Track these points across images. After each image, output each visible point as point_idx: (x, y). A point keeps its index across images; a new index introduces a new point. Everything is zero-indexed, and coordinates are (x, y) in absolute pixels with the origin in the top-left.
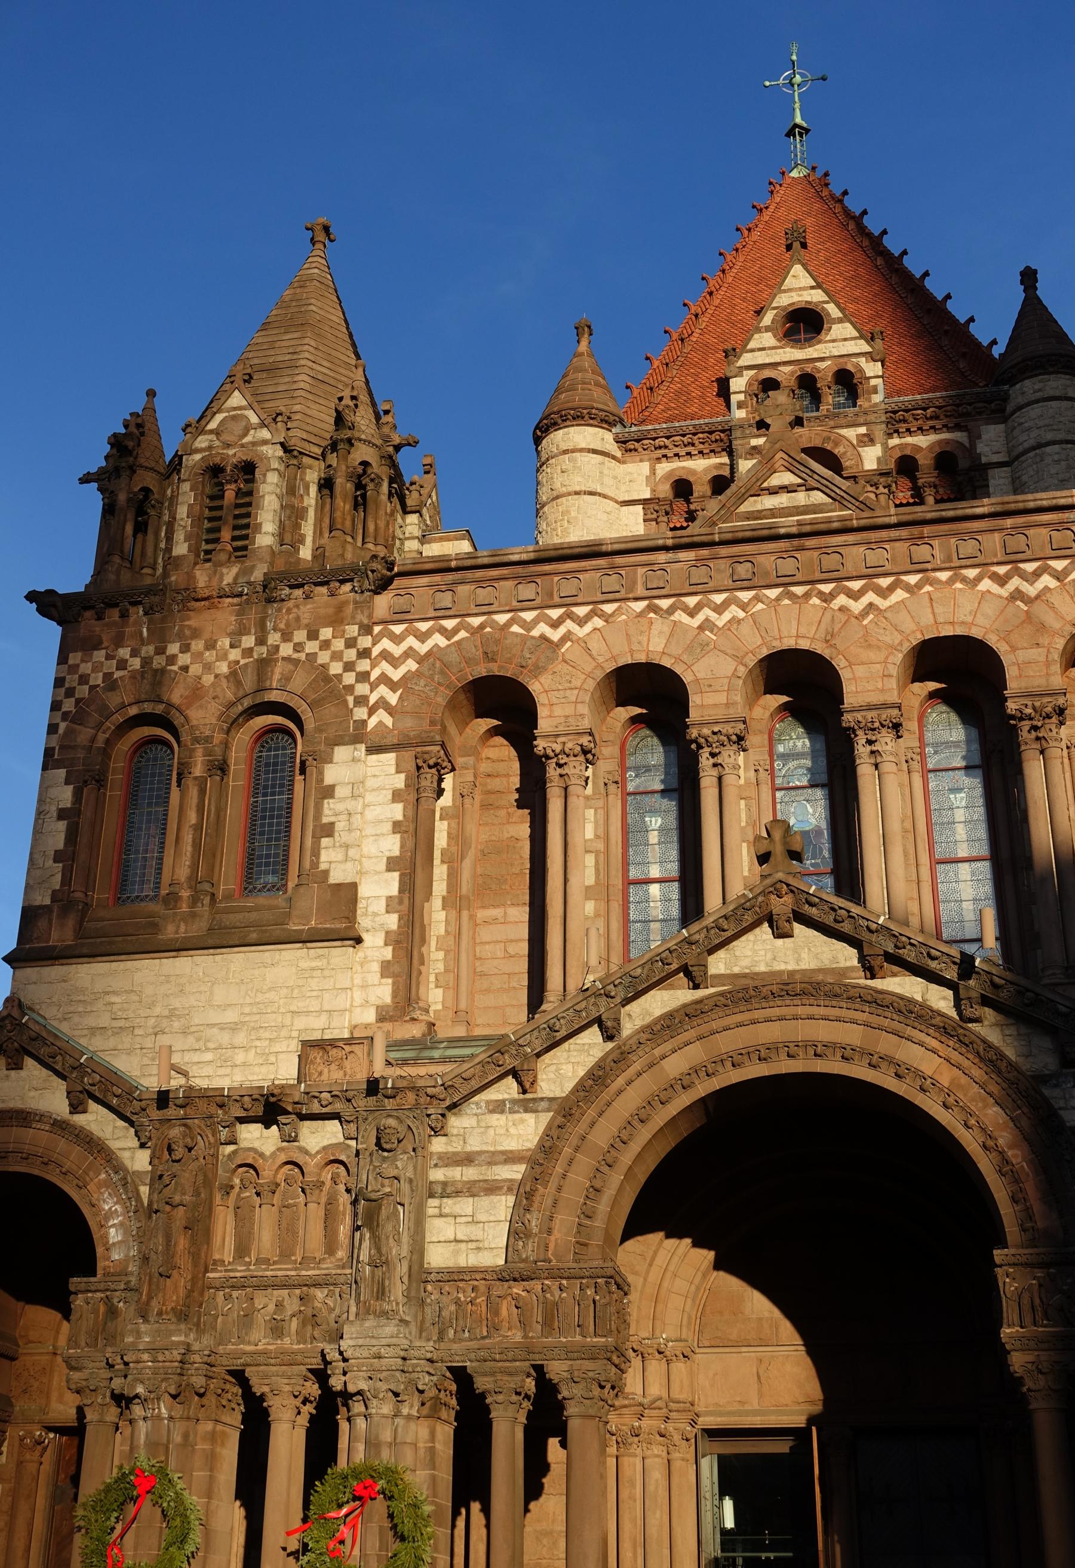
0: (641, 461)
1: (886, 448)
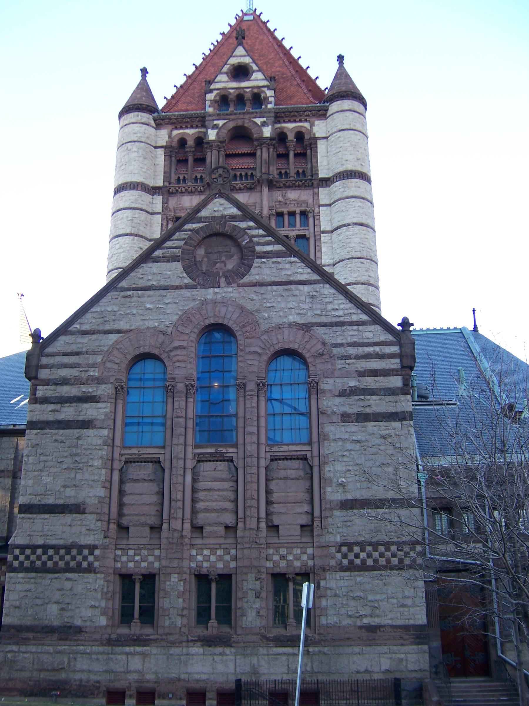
1: (274, 130)
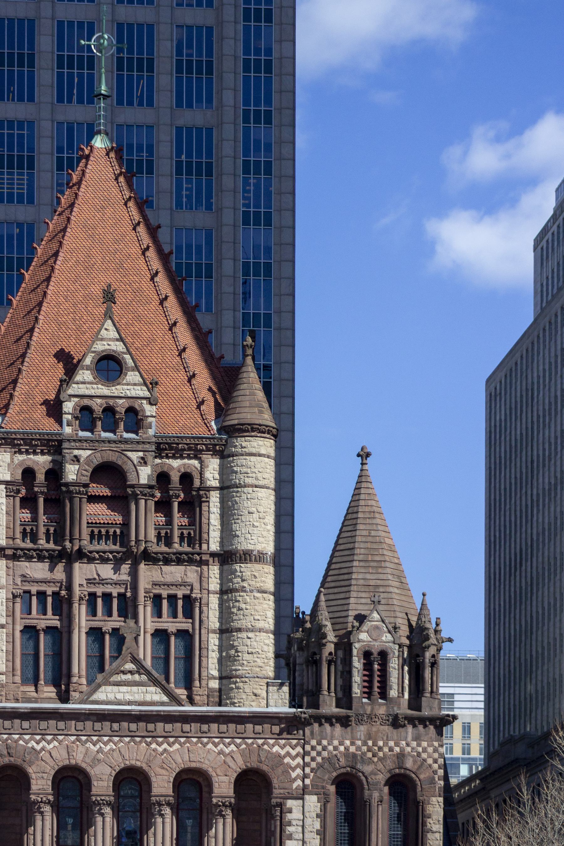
0: (5, 452)
1: (154, 466)
